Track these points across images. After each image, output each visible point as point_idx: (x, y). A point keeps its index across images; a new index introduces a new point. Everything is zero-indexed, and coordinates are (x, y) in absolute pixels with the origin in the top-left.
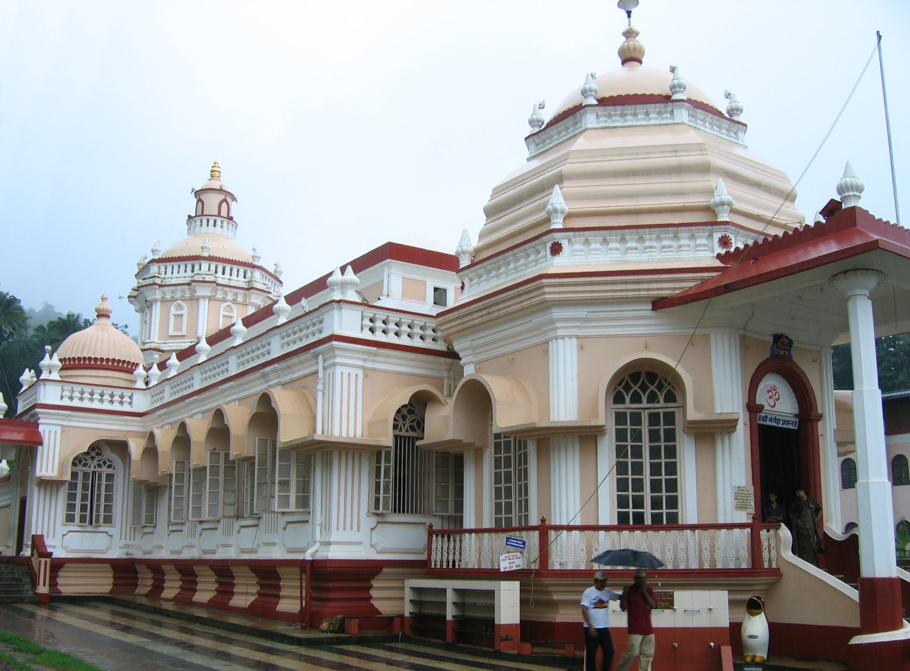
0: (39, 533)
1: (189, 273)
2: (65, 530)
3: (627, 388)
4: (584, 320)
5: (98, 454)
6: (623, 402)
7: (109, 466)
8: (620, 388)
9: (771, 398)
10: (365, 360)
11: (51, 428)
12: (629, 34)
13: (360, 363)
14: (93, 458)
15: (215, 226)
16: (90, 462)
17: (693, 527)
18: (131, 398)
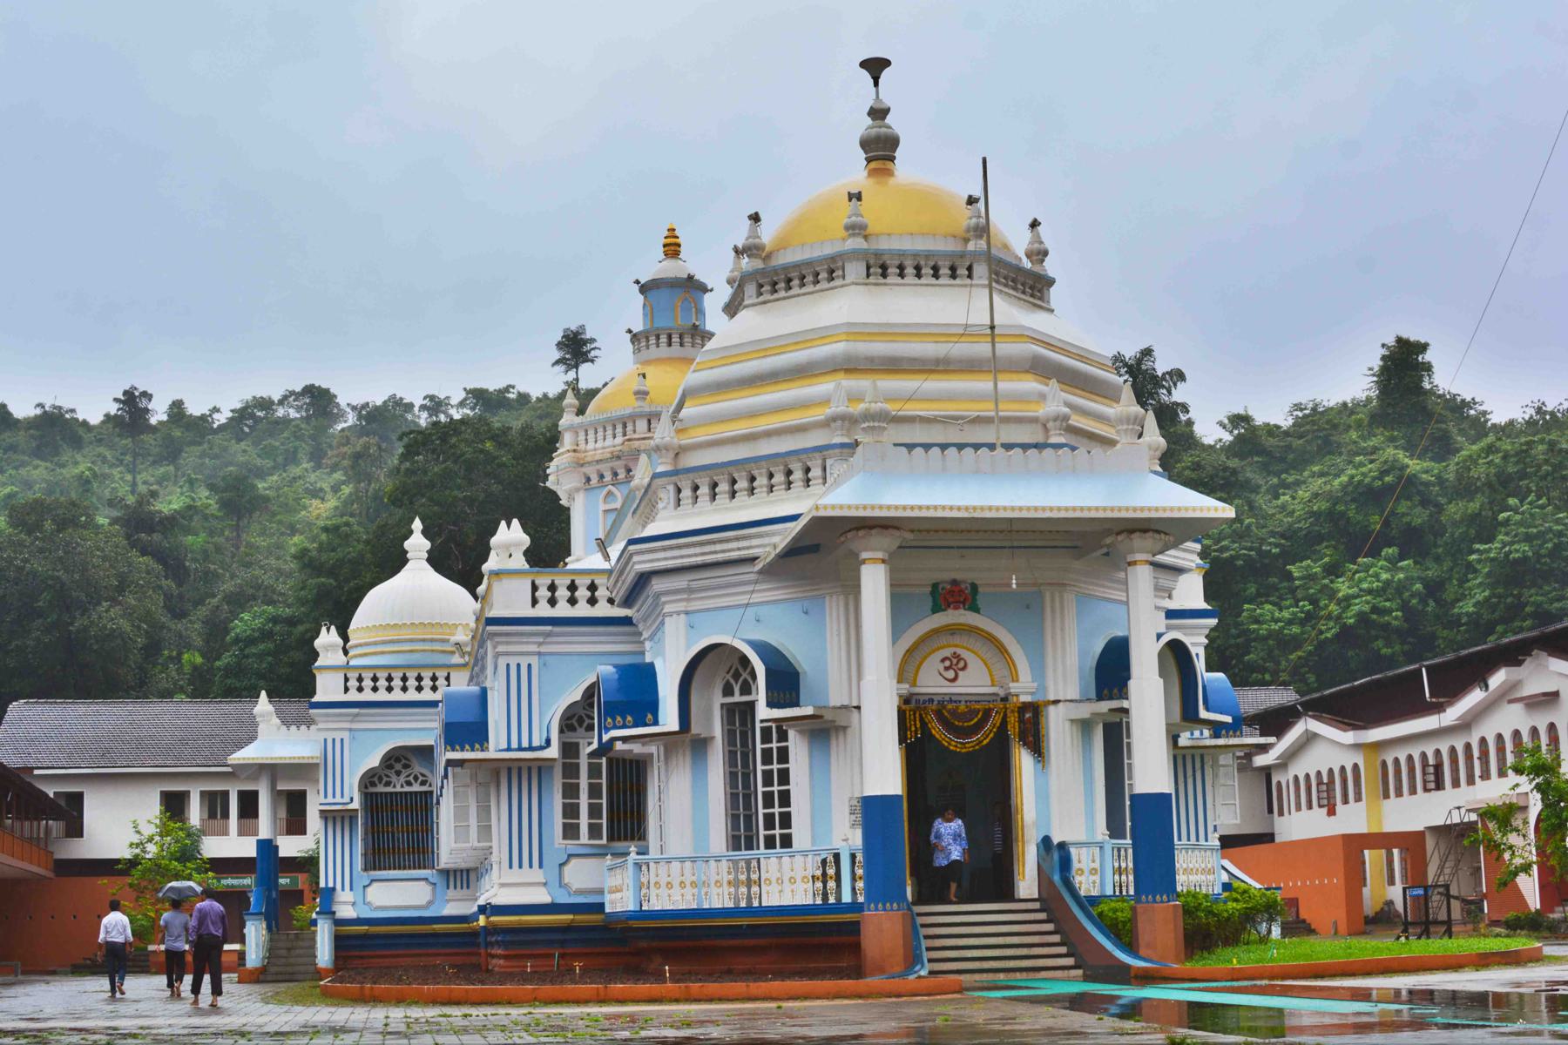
0: (331, 885)
1: (619, 439)
2: (365, 877)
3: (737, 676)
4: (690, 590)
5: (406, 766)
6: (732, 694)
7: (423, 783)
8: (729, 677)
9: (947, 669)
10: (540, 644)
11: (338, 736)
12: (878, 113)
13: (534, 648)
14: (398, 773)
15: (670, 344)
16: (394, 778)
17: (804, 853)
18: (448, 679)
